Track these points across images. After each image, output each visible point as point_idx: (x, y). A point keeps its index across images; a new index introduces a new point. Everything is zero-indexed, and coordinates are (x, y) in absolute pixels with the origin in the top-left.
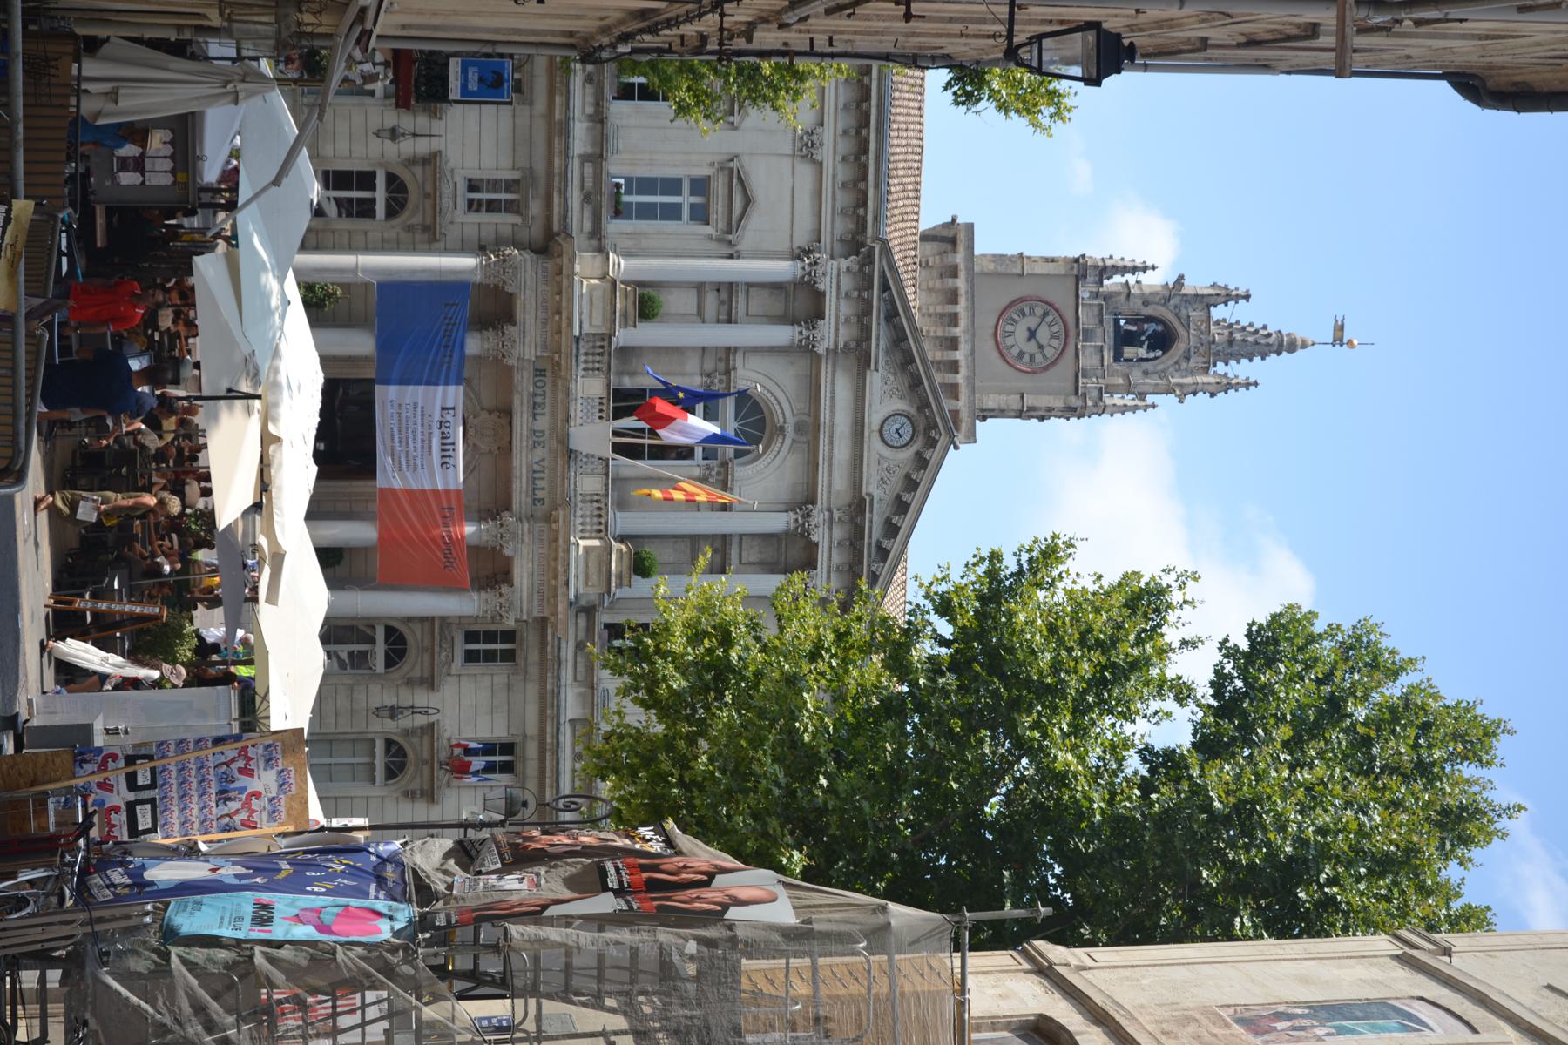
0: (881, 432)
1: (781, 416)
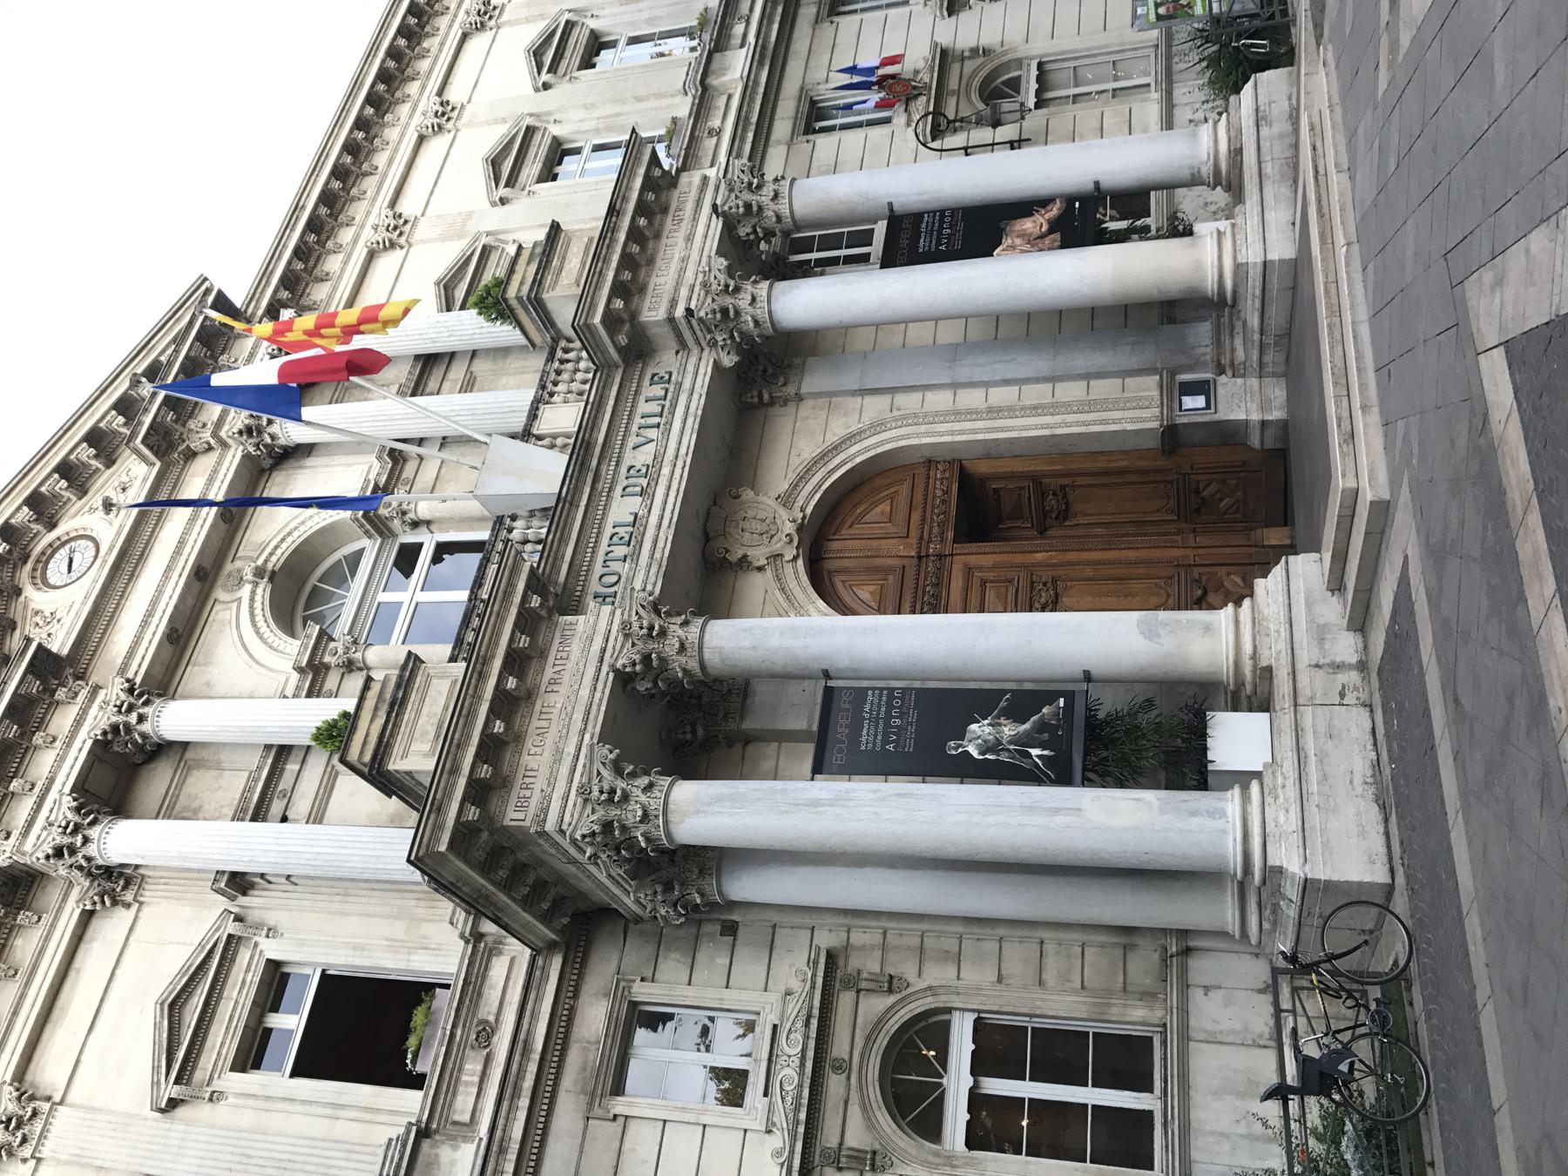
0: (96, 557)
1: (258, 598)
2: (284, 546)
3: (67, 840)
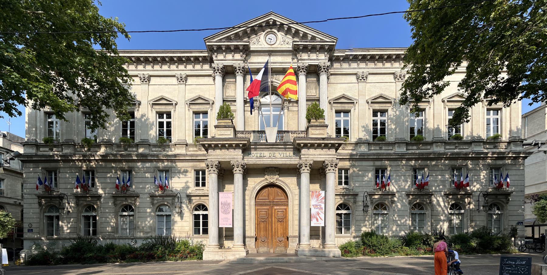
3: (216, 69)
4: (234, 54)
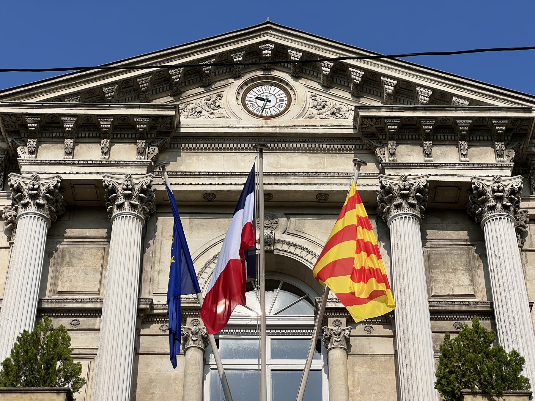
2: (298, 251)
3: (26, 192)
4: (112, 144)
